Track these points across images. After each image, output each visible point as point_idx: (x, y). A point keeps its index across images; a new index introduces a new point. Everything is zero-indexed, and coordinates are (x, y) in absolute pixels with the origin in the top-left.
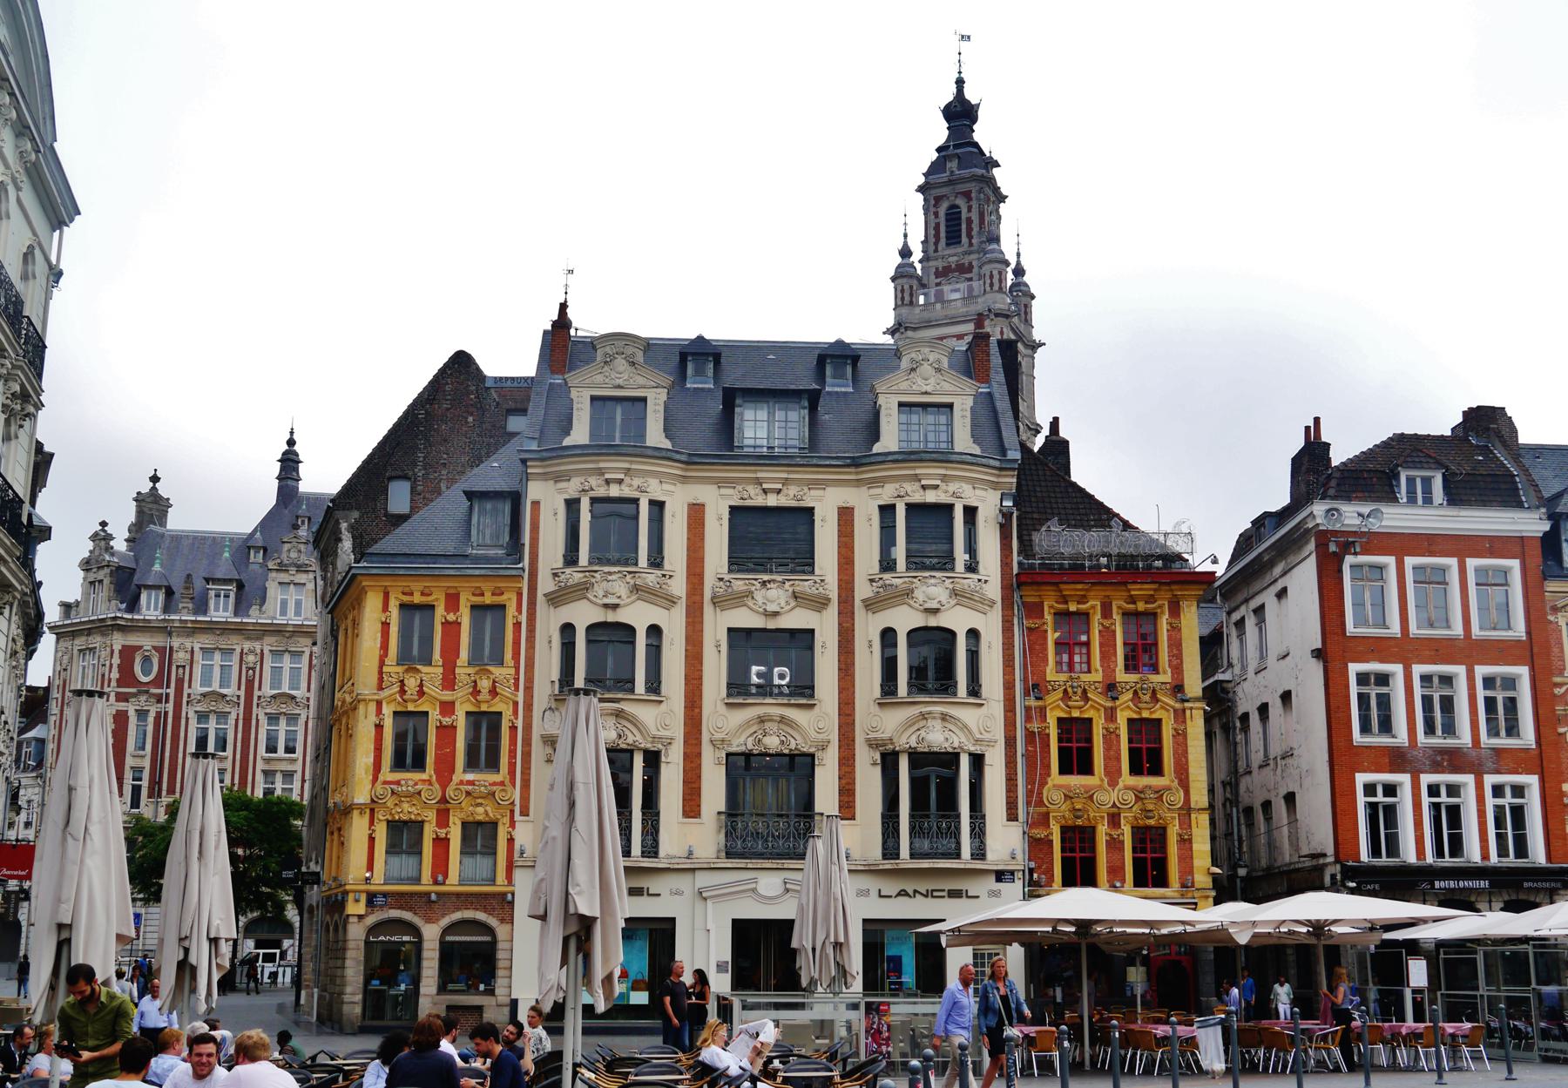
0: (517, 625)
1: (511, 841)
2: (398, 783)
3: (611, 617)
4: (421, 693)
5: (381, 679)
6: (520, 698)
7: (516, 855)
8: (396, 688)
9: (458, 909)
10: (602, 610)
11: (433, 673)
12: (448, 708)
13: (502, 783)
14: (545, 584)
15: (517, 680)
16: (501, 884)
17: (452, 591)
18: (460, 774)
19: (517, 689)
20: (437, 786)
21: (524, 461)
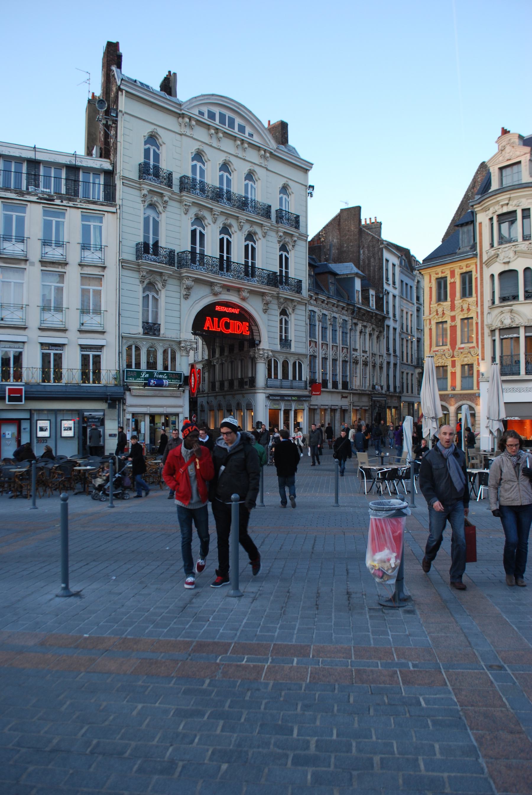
0: (476, 278)
1: (478, 371)
2: (437, 351)
3: (507, 268)
4: (443, 314)
5: (430, 310)
6: (479, 310)
7: (481, 376)
8: (435, 313)
9: (461, 400)
10: (503, 265)
11: (448, 304)
12: (453, 318)
13: (474, 347)
14: (485, 258)
15: (477, 301)
16: (475, 391)
17: (452, 269)
18: (459, 345)
19: (477, 307)
20: (451, 351)
21: (472, 206)
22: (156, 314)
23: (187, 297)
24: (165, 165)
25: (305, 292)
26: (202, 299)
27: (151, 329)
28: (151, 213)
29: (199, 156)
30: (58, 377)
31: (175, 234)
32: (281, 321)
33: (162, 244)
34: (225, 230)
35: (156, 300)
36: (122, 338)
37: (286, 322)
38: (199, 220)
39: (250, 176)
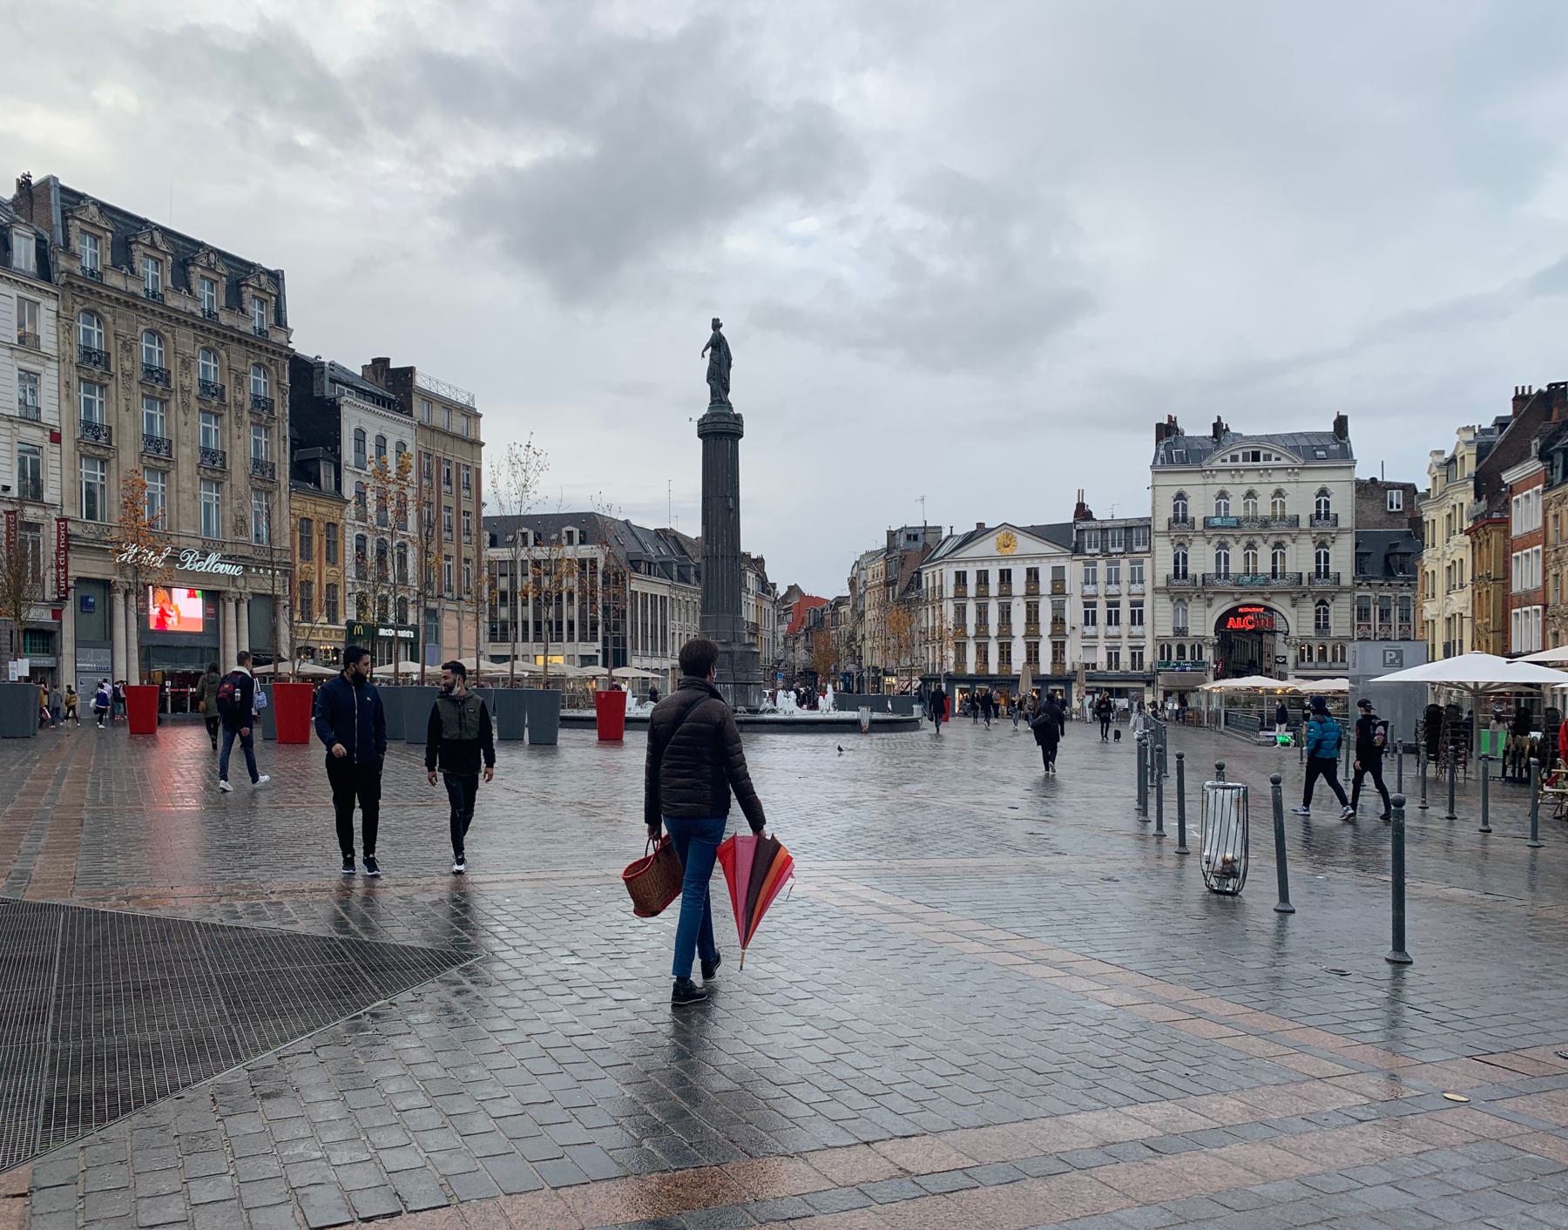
22: (1185, 620)
23: (1209, 606)
24: (1190, 515)
25: (1346, 580)
26: (1222, 605)
27: (1181, 632)
28: (1181, 551)
29: (1223, 495)
30: (1117, 667)
31: (1202, 560)
32: (1318, 611)
33: (1190, 572)
34: (1251, 545)
35: (1185, 611)
36: (1157, 640)
37: (1326, 611)
38: (1223, 545)
39: (1279, 493)
